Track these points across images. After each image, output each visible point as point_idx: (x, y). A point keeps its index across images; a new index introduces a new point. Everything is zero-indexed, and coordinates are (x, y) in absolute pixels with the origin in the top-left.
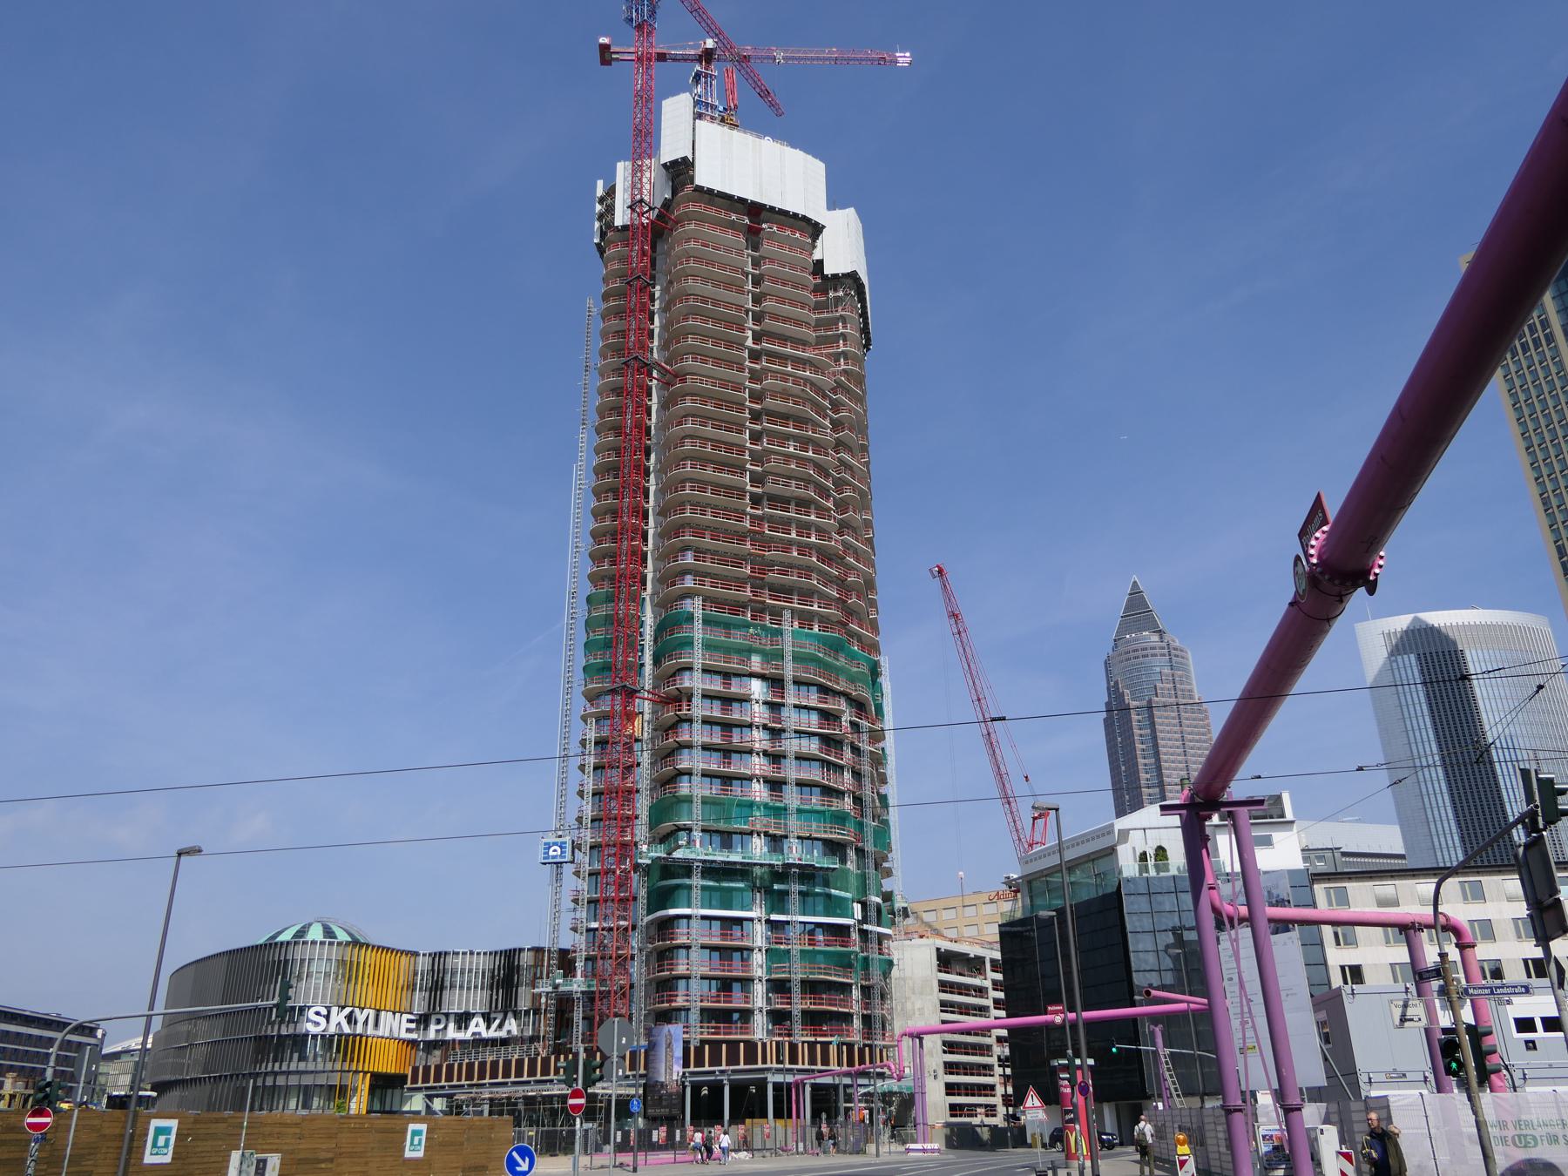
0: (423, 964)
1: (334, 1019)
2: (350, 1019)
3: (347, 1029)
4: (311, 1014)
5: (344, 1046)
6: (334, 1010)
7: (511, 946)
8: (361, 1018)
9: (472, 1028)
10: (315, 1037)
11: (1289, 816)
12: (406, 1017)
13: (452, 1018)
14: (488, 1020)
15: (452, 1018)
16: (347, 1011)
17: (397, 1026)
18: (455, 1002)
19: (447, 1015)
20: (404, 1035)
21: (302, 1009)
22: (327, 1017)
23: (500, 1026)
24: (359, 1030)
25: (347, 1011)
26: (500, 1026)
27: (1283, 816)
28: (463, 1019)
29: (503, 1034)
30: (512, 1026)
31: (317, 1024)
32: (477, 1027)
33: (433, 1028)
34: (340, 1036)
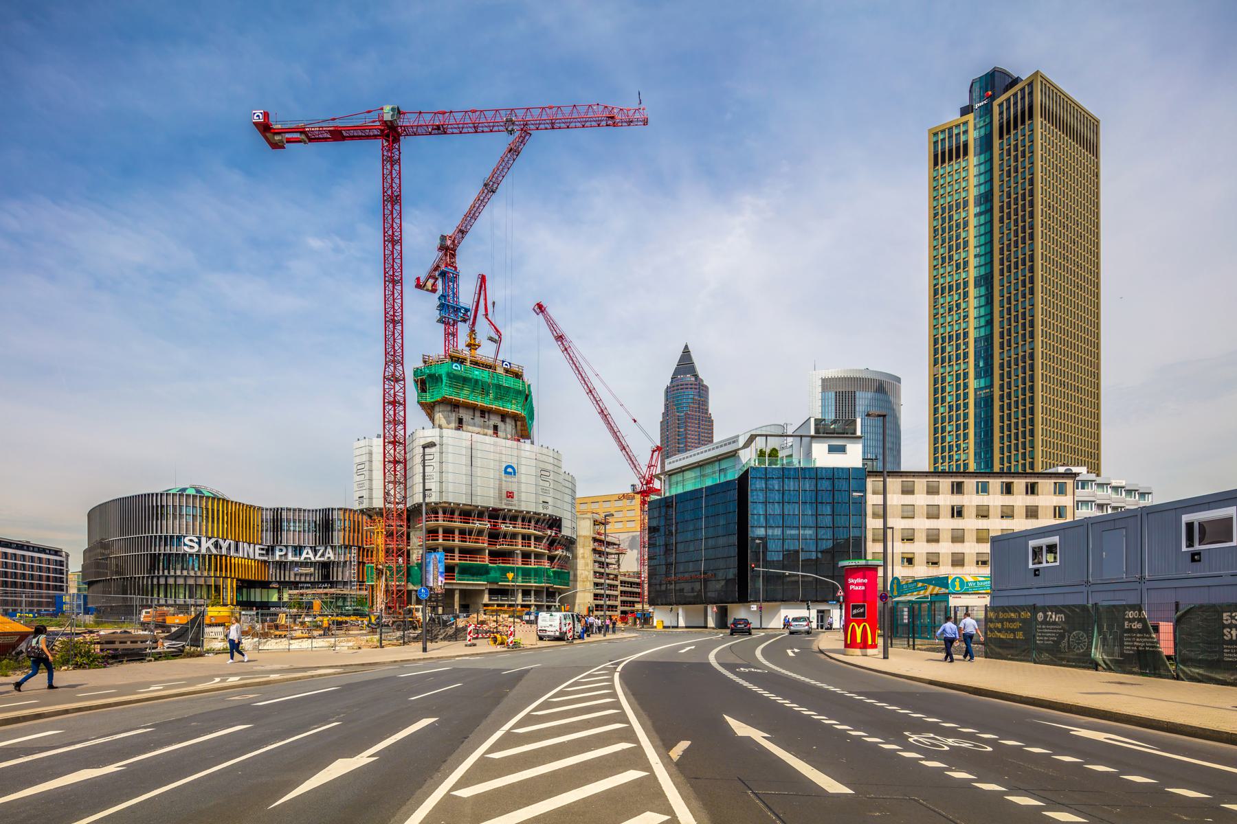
0: (269, 516)
1: (204, 545)
2: (216, 545)
3: (214, 551)
4: (186, 540)
5: (215, 561)
6: (203, 540)
7: (330, 506)
8: (225, 545)
9: (304, 555)
10: (191, 555)
11: (859, 433)
12: (257, 547)
13: (290, 549)
14: (315, 552)
15: (290, 549)
16: (213, 540)
17: (256, 552)
18: (289, 538)
19: (286, 547)
20: (257, 557)
21: (179, 538)
22: (199, 544)
23: (323, 555)
24: (224, 552)
25: (213, 540)
26: (323, 555)
27: (855, 433)
28: (298, 550)
29: (325, 559)
30: (330, 555)
31: (192, 547)
32: (307, 554)
33: (278, 553)
34: (210, 556)
